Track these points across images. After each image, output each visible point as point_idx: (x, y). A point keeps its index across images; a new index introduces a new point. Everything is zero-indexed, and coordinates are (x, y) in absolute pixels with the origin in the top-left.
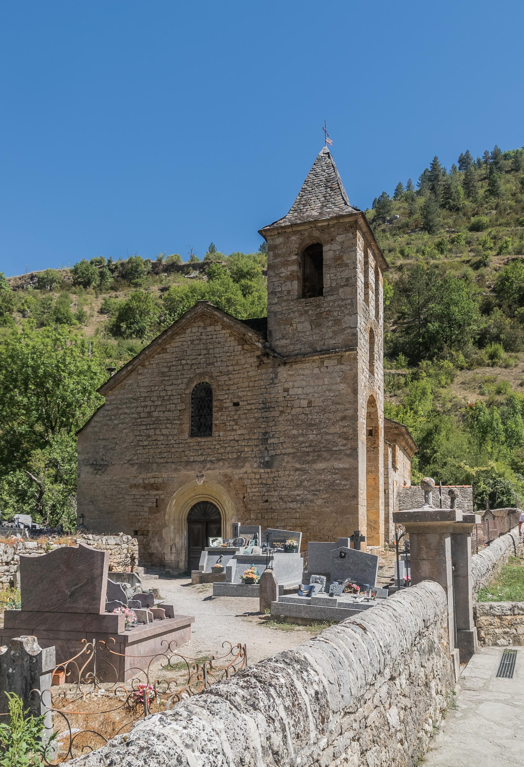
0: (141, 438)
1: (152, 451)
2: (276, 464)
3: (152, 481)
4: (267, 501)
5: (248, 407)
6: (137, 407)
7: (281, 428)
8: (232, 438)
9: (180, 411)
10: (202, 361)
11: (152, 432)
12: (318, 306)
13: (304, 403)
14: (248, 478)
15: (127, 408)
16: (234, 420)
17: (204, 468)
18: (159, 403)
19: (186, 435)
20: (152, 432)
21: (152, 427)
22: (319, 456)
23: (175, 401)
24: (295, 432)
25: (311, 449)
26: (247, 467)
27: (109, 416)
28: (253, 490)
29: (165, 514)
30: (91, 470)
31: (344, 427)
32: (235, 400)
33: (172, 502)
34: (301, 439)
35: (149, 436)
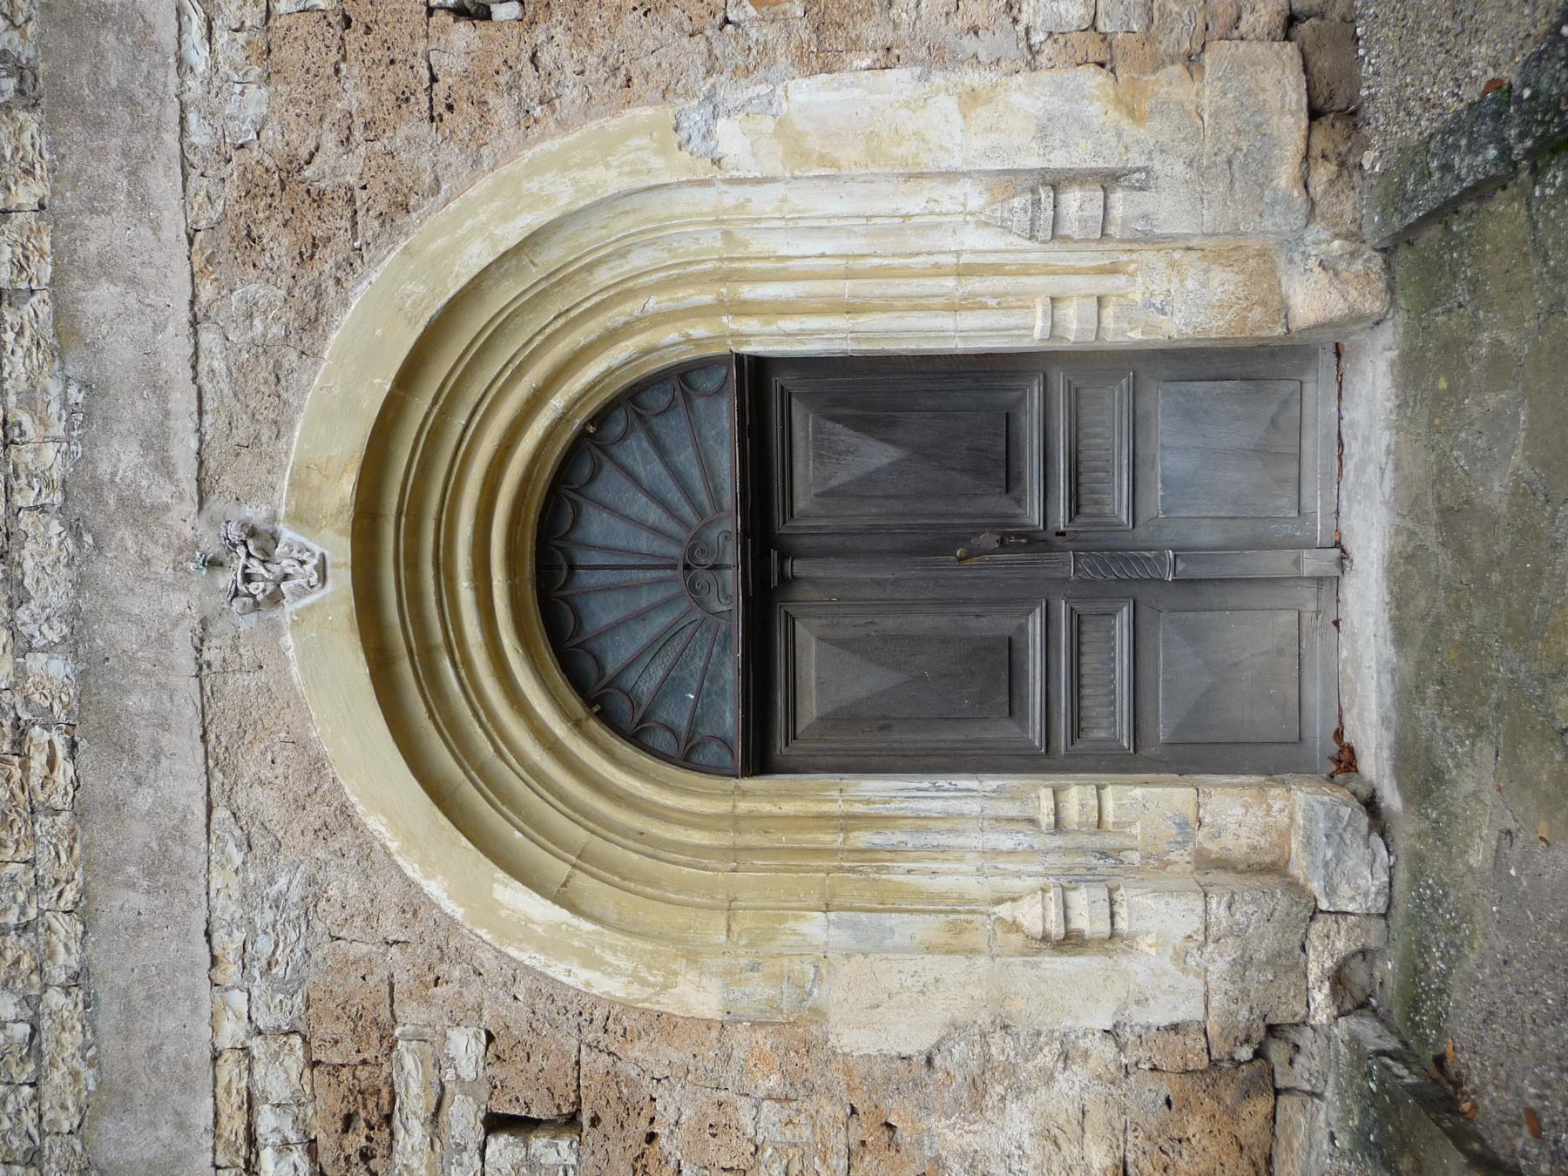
17: (143, 514)
29: (662, 1024)
33: (523, 930)
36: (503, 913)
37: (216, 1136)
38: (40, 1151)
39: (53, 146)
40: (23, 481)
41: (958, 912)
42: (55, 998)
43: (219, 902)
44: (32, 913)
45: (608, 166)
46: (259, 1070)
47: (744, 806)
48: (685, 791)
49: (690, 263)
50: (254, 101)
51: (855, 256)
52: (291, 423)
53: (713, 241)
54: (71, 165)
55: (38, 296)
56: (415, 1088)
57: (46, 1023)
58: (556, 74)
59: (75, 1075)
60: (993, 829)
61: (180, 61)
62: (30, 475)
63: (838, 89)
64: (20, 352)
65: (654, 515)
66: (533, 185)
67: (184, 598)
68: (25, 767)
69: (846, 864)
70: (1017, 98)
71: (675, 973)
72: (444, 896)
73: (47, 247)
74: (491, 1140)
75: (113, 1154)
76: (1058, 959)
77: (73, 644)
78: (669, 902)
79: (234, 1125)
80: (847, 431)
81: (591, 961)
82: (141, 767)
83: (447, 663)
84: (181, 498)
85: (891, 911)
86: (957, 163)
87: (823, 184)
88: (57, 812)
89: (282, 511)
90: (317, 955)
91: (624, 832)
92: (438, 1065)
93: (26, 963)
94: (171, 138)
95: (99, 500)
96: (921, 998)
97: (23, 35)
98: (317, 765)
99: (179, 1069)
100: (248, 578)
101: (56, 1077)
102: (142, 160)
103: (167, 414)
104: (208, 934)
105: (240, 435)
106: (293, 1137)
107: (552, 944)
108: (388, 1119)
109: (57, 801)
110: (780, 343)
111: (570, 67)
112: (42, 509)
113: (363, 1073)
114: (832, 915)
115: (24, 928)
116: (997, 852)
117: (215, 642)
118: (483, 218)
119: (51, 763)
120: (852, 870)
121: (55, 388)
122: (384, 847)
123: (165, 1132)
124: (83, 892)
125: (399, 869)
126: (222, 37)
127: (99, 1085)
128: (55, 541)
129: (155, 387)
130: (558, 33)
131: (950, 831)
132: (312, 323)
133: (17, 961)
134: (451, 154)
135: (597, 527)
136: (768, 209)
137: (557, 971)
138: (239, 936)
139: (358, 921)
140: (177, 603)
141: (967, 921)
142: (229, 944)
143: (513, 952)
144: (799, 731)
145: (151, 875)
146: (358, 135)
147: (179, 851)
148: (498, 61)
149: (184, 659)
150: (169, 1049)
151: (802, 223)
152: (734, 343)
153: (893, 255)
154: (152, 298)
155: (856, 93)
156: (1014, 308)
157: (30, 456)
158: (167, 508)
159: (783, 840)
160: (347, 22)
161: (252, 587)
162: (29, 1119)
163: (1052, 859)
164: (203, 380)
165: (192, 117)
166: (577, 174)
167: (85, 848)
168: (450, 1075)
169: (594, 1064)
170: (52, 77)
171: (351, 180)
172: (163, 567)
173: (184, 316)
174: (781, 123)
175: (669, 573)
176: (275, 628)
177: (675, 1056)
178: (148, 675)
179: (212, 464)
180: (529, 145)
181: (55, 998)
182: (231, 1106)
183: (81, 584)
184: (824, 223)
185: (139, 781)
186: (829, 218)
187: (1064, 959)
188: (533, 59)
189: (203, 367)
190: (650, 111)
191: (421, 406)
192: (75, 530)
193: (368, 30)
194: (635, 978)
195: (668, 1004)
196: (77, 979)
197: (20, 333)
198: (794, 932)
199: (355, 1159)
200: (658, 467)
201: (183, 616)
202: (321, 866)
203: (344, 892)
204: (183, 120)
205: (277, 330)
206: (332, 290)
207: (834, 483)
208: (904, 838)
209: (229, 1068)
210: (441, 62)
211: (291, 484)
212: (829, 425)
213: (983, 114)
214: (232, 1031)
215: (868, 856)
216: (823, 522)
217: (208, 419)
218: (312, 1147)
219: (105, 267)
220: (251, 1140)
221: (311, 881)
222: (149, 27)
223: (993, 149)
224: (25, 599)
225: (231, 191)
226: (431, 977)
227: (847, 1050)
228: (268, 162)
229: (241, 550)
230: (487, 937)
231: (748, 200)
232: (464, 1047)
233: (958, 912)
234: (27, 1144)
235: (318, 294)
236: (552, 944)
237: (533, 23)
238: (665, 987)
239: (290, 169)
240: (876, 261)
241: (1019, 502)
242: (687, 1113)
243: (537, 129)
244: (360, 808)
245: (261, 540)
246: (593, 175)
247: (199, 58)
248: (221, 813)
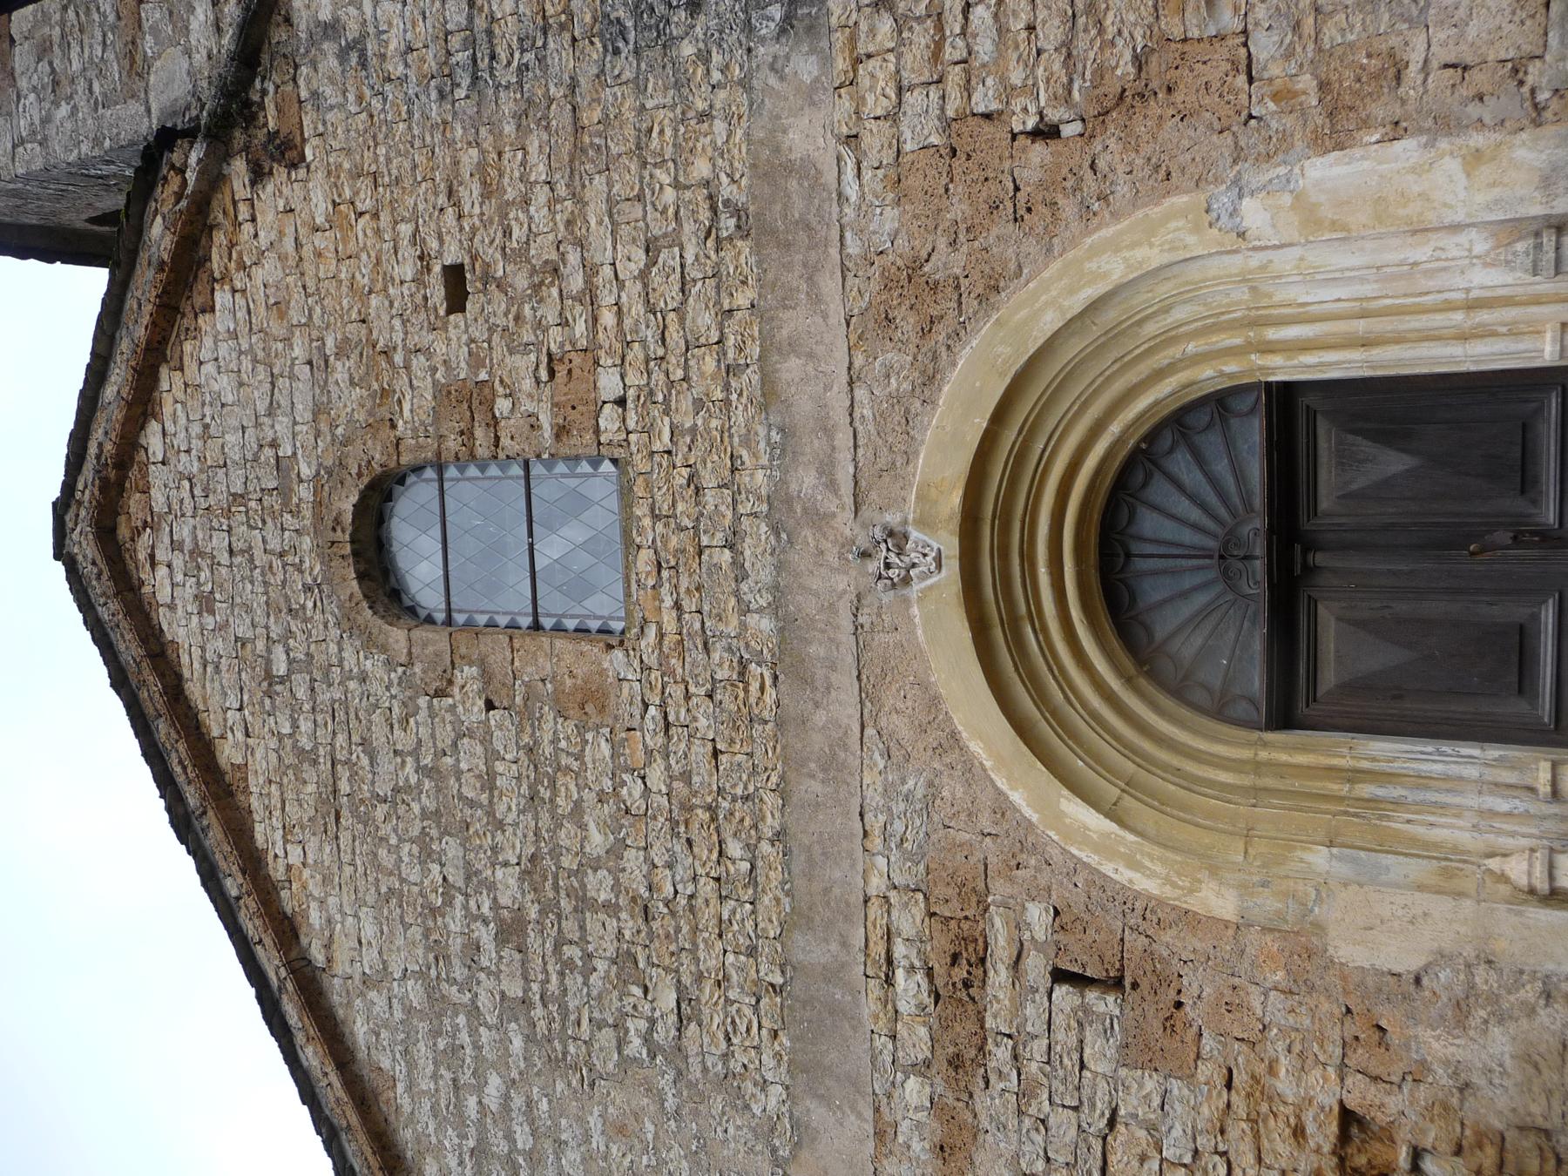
0: (635, 1026)
3: (909, 989)
5: (470, 194)
6: (474, 1011)
9: (490, 706)
11: (603, 935)
14: (892, 117)
15: (479, 1088)
16: (537, 287)
17: (819, 519)
20: (603, 935)
21: (570, 927)
23: (445, 735)
28: (985, 48)
29: (1189, 919)
33: (1081, 834)
36: (1068, 821)
37: (867, 955)
38: (756, 948)
39: (759, 263)
40: (743, 496)
41: (1451, 860)
42: (765, 847)
43: (869, 793)
44: (751, 789)
45: (1151, 245)
46: (895, 913)
47: (1263, 755)
48: (1215, 739)
49: (1223, 313)
50: (888, 219)
51: (1368, 299)
52: (917, 453)
53: (1242, 294)
54: (770, 276)
55: (751, 368)
56: (1002, 942)
57: (760, 863)
58: (1110, 175)
59: (778, 900)
60: (1491, 793)
61: (840, 195)
62: (748, 492)
63: (1348, 164)
64: (741, 408)
65: (1195, 515)
66: (1093, 265)
67: (846, 579)
68: (746, 691)
69: (1352, 810)
70: (1521, 153)
71: (1200, 882)
72: (1024, 804)
73: (756, 334)
74: (1056, 987)
75: (801, 957)
76: (1541, 911)
77: (775, 608)
78: (1197, 825)
79: (878, 949)
80: (1365, 442)
81: (1134, 865)
82: (818, 696)
83: (1029, 630)
84: (843, 508)
85: (1388, 852)
86: (1460, 216)
87: (1336, 244)
88: (766, 722)
89: (911, 517)
90: (934, 837)
91: (1166, 767)
92: (1018, 927)
93: (747, 822)
94: (834, 252)
95: (791, 509)
96: (1411, 927)
97: (739, 187)
98: (935, 702)
99: (843, 905)
100: (888, 566)
101: (766, 900)
102: (816, 269)
103: (834, 448)
104: (861, 815)
105: (882, 462)
106: (917, 964)
107: (1104, 847)
108: (983, 961)
109: (766, 715)
110: (1303, 372)
111: (1121, 169)
112: (755, 515)
113: (965, 925)
114: (1335, 850)
115: (746, 798)
116: (1493, 814)
117: (866, 610)
118: (1054, 293)
119: (762, 689)
120: (1356, 815)
121: (762, 431)
122: (981, 763)
123: (834, 947)
124: (782, 777)
125: (992, 781)
126: (867, 175)
127: (793, 909)
128: (763, 537)
129: (825, 429)
130: (1112, 143)
131: (1448, 791)
132: (930, 379)
133: (742, 820)
134: (1031, 246)
135: (1149, 523)
136: (1288, 268)
137: (1108, 868)
138: (882, 818)
139: (963, 816)
140: (841, 582)
141: (1457, 869)
142: (875, 822)
143: (1075, 851)
144: (1318, 695)
145: (825, 770)
146: (962, 237)
147: (842, 755)
148: (1065, 171)
149: (846, 622)
150: (837, 891)
151: (1318, 277)
152: (1262, 374)
153: (1405, 295)
154: (823, 367)
155: (1366, 164)
156: (1524, 333)
157: (748, 479)
158: (834, 515)
159: (1297, 785)
160: (954, 152)
161: (891, 572)
162: (749, 925)
163: (1548, 825)
164: (857, 424)
165: (848, 235)
166: (1127, 254)
167: (783, 748)
168: (1027, 935)
169: (1135, 943)
170: (758, 215)
171: (958, 271)
172: (832, 558)
173: (844, 379)
174: (1298, 197)
175: (1208, 561)
176: (906, 601)
177: (1198, 945)
178: (823, 632)
179: (863, 483)
180: (1090, 233)
181: (765, 847)
182: (877, 935)
183: (779, 567)
184: (1337, 275)
185: (817, 705)
186: (1342, 270)
187: (1548, 911)
188: (1093, 166)
189: (857, 415)
190: (1185, 198)
191: (1009, 437)
192: (776, 530)
193: (969, 157)
194: (1167, 881)
195: (1193, 904)
196: (779, 836)
197: (740, 395)
198: (1302, 860)
199: (959, 985)
200: (1199, 476)
201: (845, 592)
202: (938, 774)
203: (953, 794)
204: (842, 237)
205: (906, 386)
206: (944, 355)
207: (1354, 487)
208: (1404, 792)
209: (875, 909)
210: (1023, 175)
211: (917, 498)
212: (1350, 437)
213: (1486, 172)
214: (877, 884)
215: (1372, 805)
216: (1343, 520)
217: (861, 452)
218: (930, 972)
219: (793, 346)
220: (890, 961)
221: (930, 784)
222: (819, 172)
223: (1496, 202)
224: (745, 577)
225: (875, 286)
226: (1013, 863)
227: (1343, 961)
228: (900, 262)
229: (883, 546)
230: (1055, 838)
231: (1271, 261)
232: (1038, 917)
233: (1451, 860)
234: (748, 942)
235: (935, 358)
236: (1104, 847)
237: (1092, 136)
238: (1191, 891)
239: (915, 266)
240: (1388, 302)
241: (1535, 502)
242: (1207, 990)
243: (1095, 221)
244: (964, 735)
245: (896, 538)
246: (1139, 253)
247: (852, 191)
248: (870, 731)
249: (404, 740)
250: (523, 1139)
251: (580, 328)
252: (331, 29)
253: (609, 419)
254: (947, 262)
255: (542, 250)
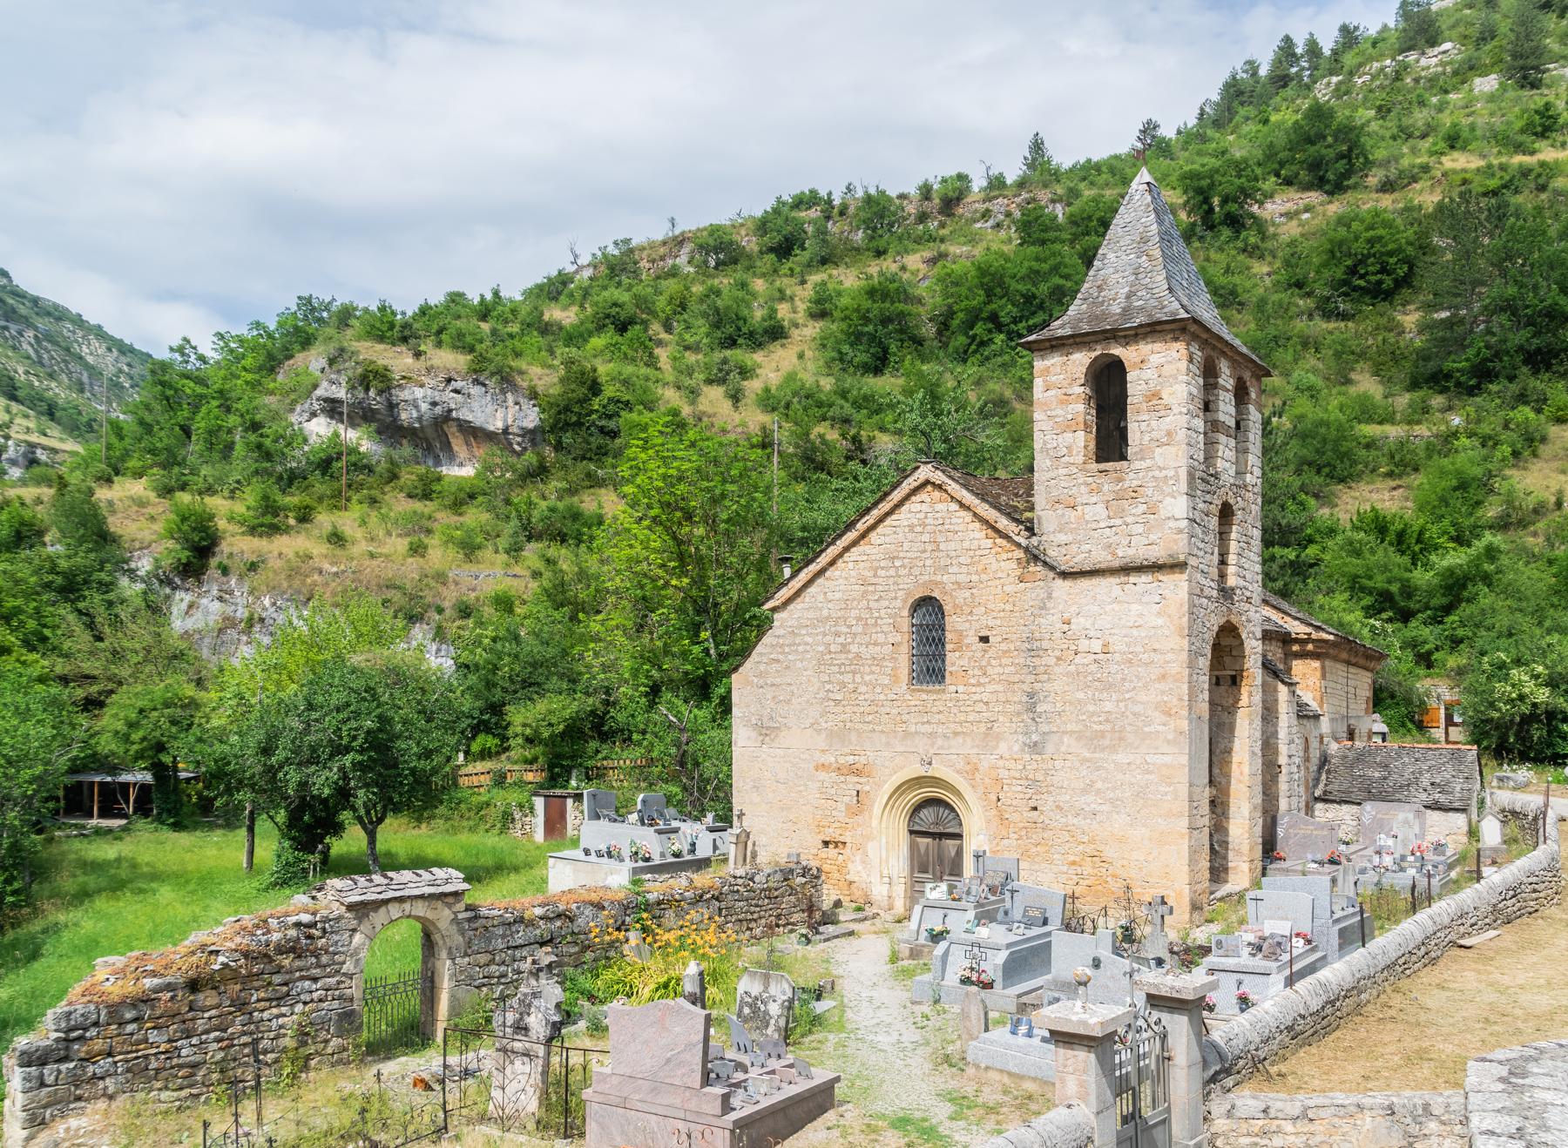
1: (848, 709)
2: (1050, 748)
3: (851, 759)
4: (1035, 809)
5: (1004, 646)
6: (825, 635)
7: (1057, 686)
8: (976, 697)
10: (928, 562)
11: (848, 678)
12: (1120, 480)
13: (1096, 646)
17: (933, 744)
18: (860, 629)
19: (903, 686)
20: (848, 678)
22: (1121, 739)
23: (885, 629)
24: (1080, 695)
25: (1108, 727)
26: (1003, 748)
27: (782, 646)
30: (754, 734)
31: (1163, 692)
32: (983, 634)
34: (1091, 708)
35: (843, 685)
232: (867, 788)
249: (883, 612)
250: (801, 648)
251: (972, 681)
252: (1050, 597)
253: (953, 688)
254: (978, 776)
255: (990, 670)
